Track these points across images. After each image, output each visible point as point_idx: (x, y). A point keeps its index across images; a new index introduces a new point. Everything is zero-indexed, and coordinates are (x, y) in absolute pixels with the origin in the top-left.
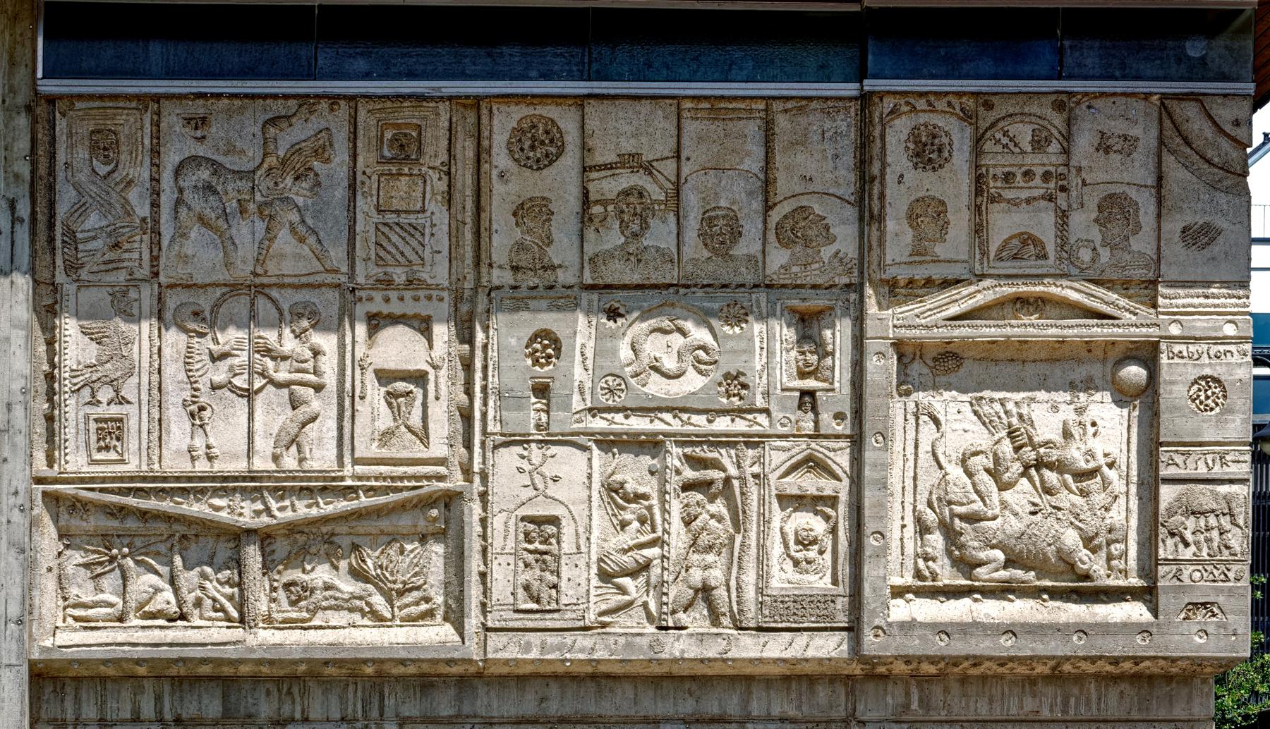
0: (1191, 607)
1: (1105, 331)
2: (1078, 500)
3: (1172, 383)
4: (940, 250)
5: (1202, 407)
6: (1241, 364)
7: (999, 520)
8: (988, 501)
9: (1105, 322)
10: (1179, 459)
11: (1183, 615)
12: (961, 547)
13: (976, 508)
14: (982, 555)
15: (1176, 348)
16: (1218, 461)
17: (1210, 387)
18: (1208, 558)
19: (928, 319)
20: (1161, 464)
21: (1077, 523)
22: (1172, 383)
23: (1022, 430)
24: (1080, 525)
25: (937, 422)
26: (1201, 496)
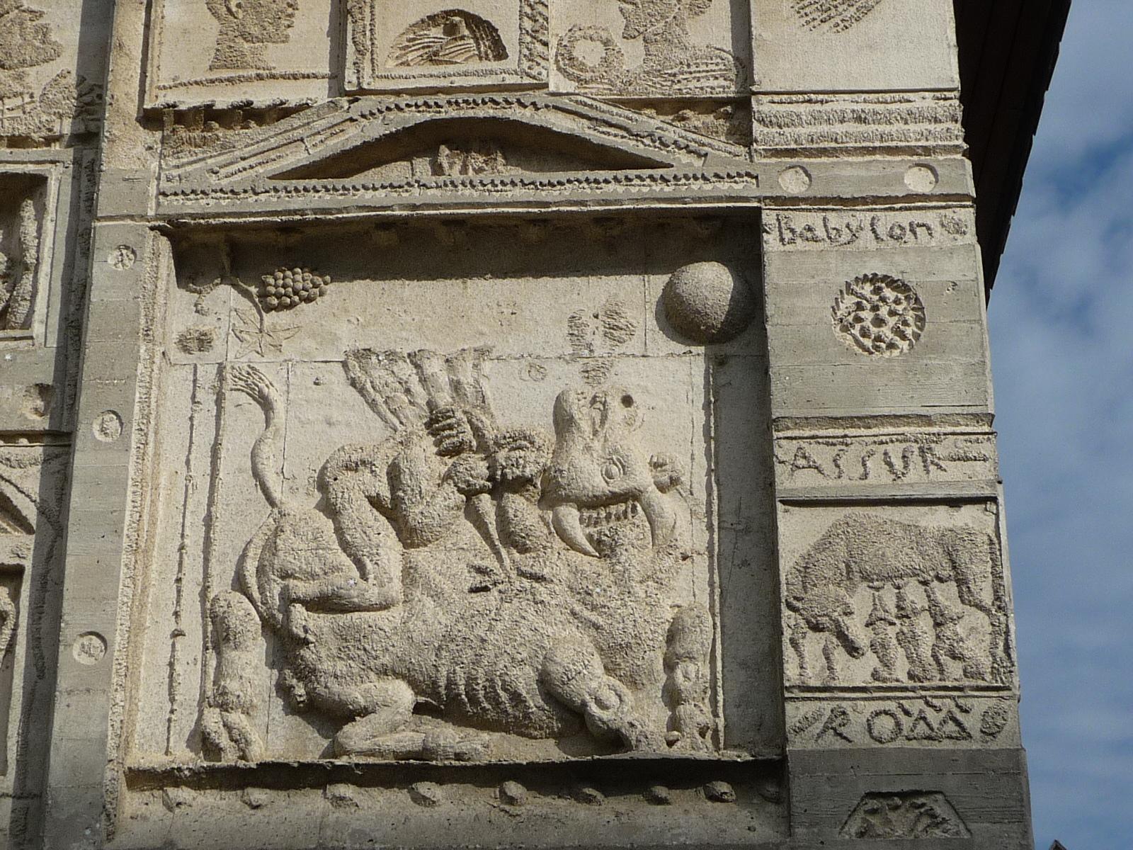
0: (873, 804)
1: (634, 190)
2: (590, 564)
3: (798, 291)
4: (275, 56)
5: (868, 343)
6: (952, 251)
7: (397, 613)
8: (369, 566)
9: (632, 173)
10: (820, 453)
11: (854, 827)
12: (307, 674)
13: (342, 582)
14: (356, 694)
15: (800, 220)
16: (915, 458)
17: (883, 299)
18: (910, 684)
19: (237, 178)
20: (778, 469)
21: (586, 613)
22: (798, 291)
23: (459, 414)
24: (594, 617)
25: (265, 403)
26: (884, 538)
